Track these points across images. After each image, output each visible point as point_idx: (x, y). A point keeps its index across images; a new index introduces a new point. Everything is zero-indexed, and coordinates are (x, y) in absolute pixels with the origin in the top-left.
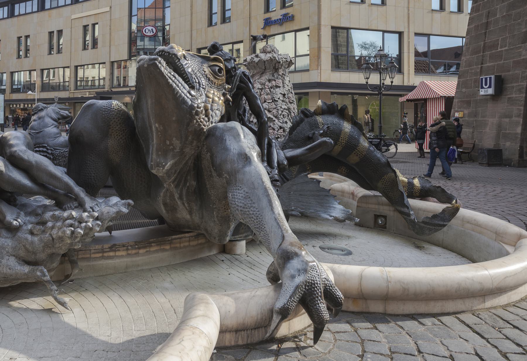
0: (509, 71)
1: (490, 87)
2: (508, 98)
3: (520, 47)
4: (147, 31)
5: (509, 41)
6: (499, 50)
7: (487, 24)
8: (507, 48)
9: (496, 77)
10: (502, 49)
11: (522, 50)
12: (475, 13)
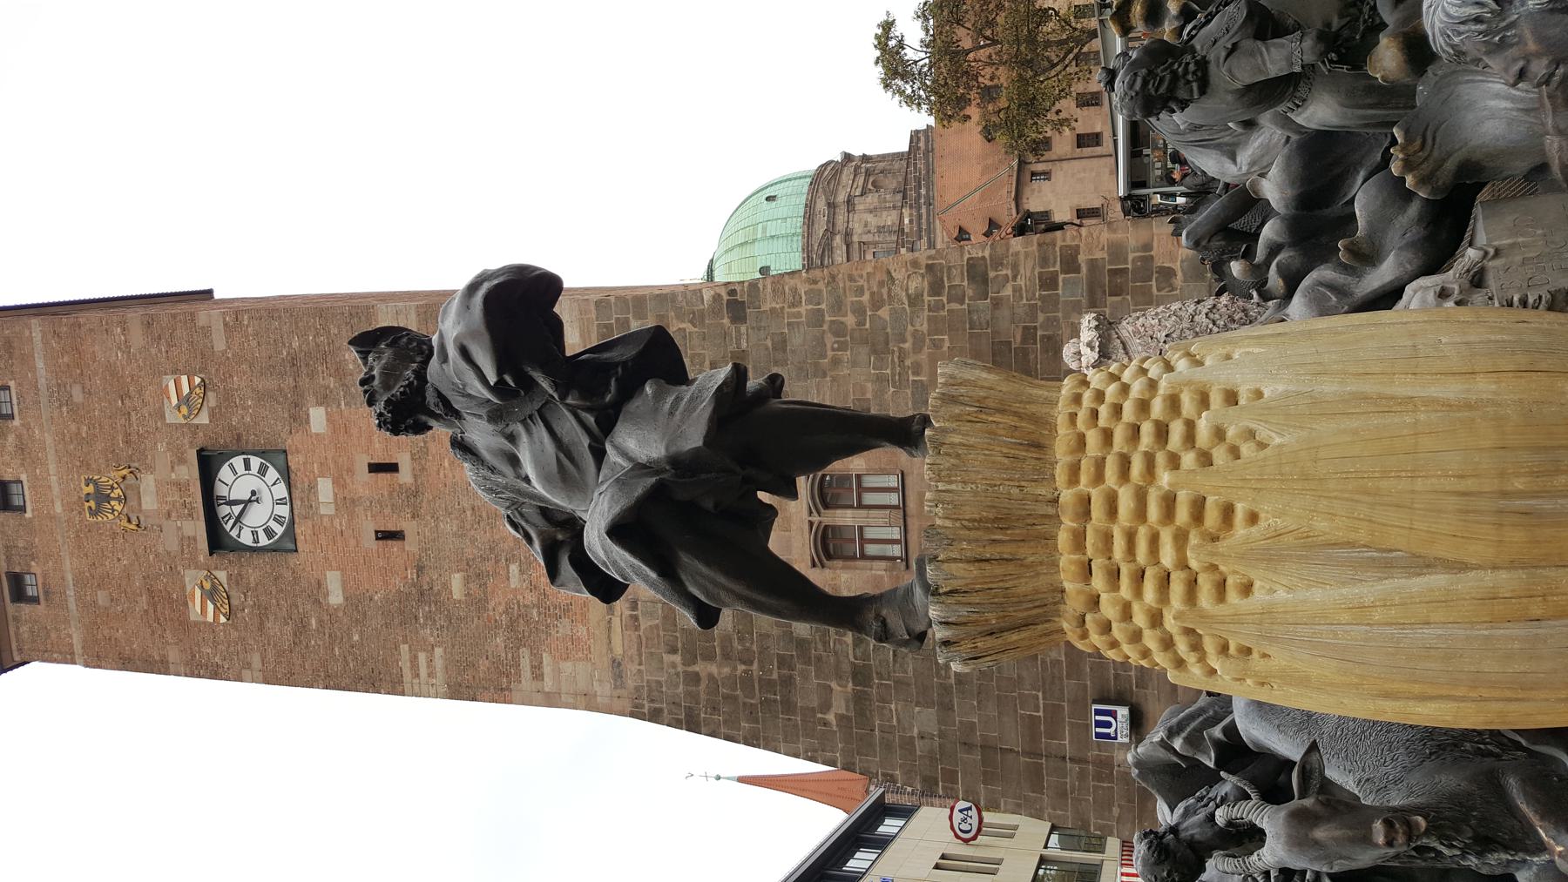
0: (1086, 686)
1: (1113, 714)
2: (1137, 687)
3: (1043, 662)
4: (965, 827)
5: (1028, 690)
6: (1041, 714)
7: (986, 748)
8: (1040, 695)
9: (1095, 702)
10: (1042, 706)
11: (1048, 659)
12: (957, 784)
